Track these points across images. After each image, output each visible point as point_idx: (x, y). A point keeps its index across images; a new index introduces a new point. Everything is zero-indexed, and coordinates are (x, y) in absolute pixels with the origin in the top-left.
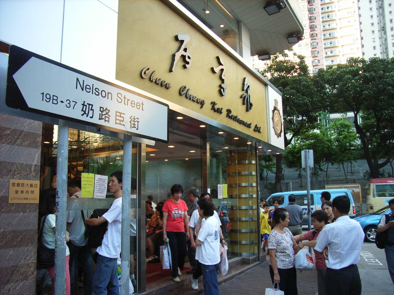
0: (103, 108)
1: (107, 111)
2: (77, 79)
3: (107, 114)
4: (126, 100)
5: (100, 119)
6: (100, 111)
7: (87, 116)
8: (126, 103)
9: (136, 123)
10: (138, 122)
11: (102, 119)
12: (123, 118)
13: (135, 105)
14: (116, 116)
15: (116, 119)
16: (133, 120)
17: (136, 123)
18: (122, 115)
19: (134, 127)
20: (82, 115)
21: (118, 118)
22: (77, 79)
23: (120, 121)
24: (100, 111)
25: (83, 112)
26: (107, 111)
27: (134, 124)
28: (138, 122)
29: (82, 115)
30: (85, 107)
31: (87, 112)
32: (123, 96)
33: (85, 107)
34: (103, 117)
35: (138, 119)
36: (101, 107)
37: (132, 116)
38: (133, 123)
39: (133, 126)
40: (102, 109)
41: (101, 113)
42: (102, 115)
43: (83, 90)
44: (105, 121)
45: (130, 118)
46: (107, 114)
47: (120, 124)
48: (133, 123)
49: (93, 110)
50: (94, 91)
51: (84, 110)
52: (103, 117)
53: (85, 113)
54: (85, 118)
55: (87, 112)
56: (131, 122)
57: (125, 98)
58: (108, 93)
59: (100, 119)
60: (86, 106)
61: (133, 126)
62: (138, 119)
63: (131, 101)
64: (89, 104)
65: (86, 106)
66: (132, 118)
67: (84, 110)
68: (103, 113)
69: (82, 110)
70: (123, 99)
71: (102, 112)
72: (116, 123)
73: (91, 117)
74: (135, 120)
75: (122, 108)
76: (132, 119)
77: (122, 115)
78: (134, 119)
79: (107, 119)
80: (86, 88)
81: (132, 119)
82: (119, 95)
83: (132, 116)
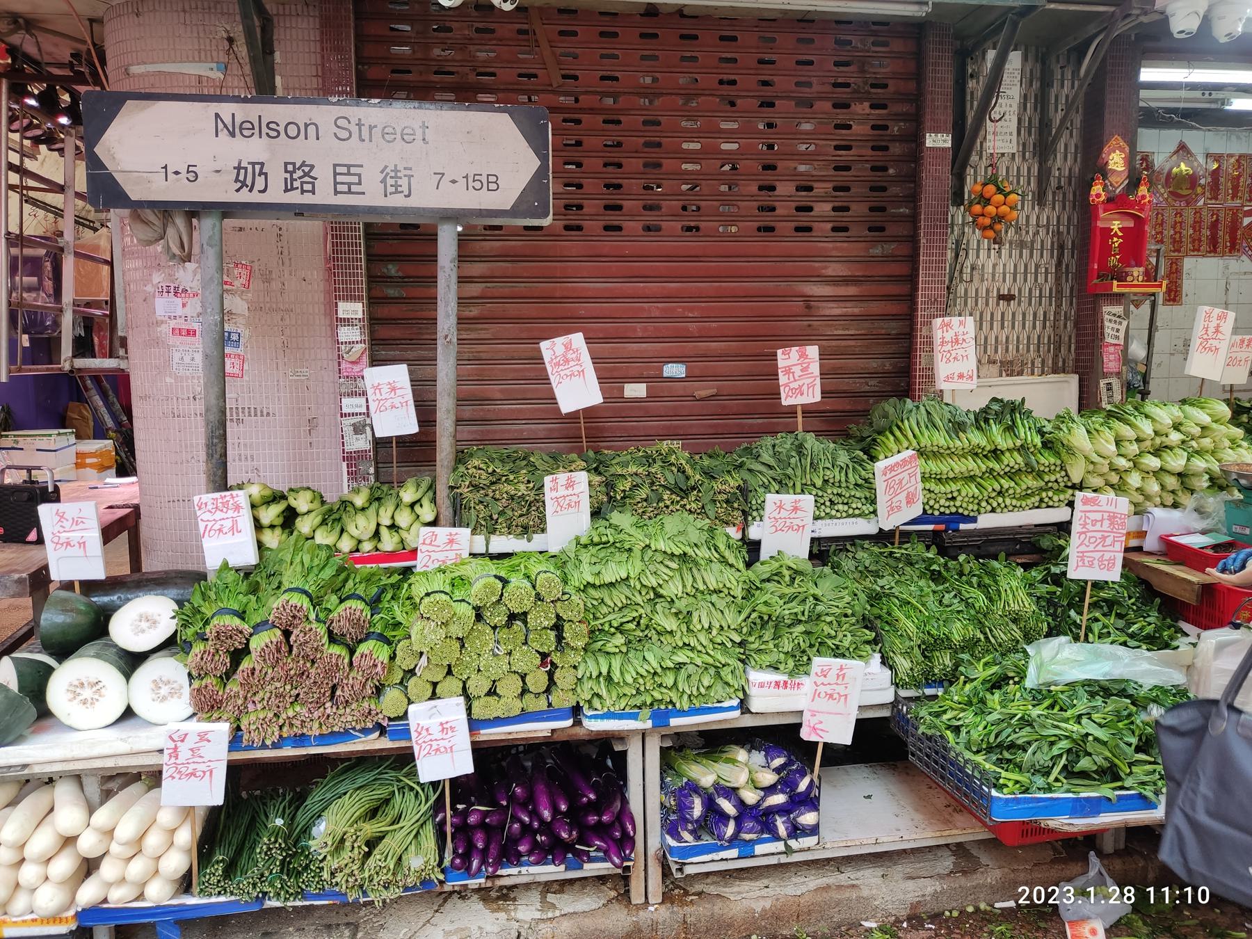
0: (294, 164)
1: (307, 169)
2: (217, 115)
3: (306, 174)
4: (365, 130)
5: (286, 190)
6: (286, 171)
7: (250, 191)
8: (365, 134)
9: (404, 182)
10: (410, 177)
11: (293, 189)
12: (359, 175)
13: (398, 136)
14: (335, 174)
15: (336, 183)
16: (393, 174)
18: (353, 170)
19: (397, 192)
20: (238, 190)
21: (339, 179)
22: (217, 115)
23: (349, 184)
24: (286, 171)
25: (239, 185)
26: (307, 169)
27: (396, 186)
28: (410, 177)
29: (238, 190)
30: (242, 171)
31: (249, 182)
32: (354, 121)
33: (242, 171)
34: (297, 184)
36: (286, 164)
37: (386, 167)
38: (392, 182)
39: (393, 189)
40: (290, 168)
41: (288, 175)
42: (293, 180)
43: (233, 134)
44: (303, 192)
45: (382, 172)
46: (306, 174)
47: (350, 192)
48: (390, 182)
49: (266, 174)
50: (264, 130)
51: (242, 178)
52: (297, 184)
53: (244, 184)
54: (245, 197)
55: (249, 182)
56: (384, 181)
57: (359, 125)
58: (306, 126)
59: (286, 190)
60: (246, 169)
64: (253, 164)
65: (246, 169)
66: (388, 170)
67: (242, 178)
68: (295, 176)
69: (237, 180)
70: (355, 129)
71: (291, 173)
72: (336, 192)
73: (264, 191)
75: (350, 152)
77: (353, 170)
78: (396, 171)
79: (308, 187)
80: (241, 129)
82: (340, 122)
83: (386, 167)
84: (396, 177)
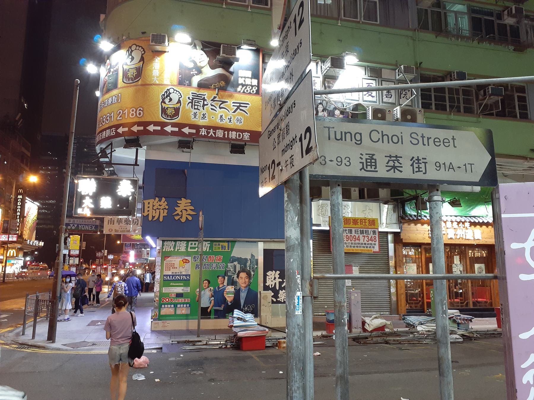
9: (422, 166)
10: (425, 163)
17: (422, 166)
28: (425, 163)
35: (425, 159)
37: (413, 158)
45: (411, 160)
48: (416, 165)
61: (417, 170)
62: (425, 159)
63: (433, 139)
66: (414, 159)
74: (420, 162)
76: (414, 161)
78: (418, 159)
81: (414, 161)
83: (413, 158)
84: (418, 163)
